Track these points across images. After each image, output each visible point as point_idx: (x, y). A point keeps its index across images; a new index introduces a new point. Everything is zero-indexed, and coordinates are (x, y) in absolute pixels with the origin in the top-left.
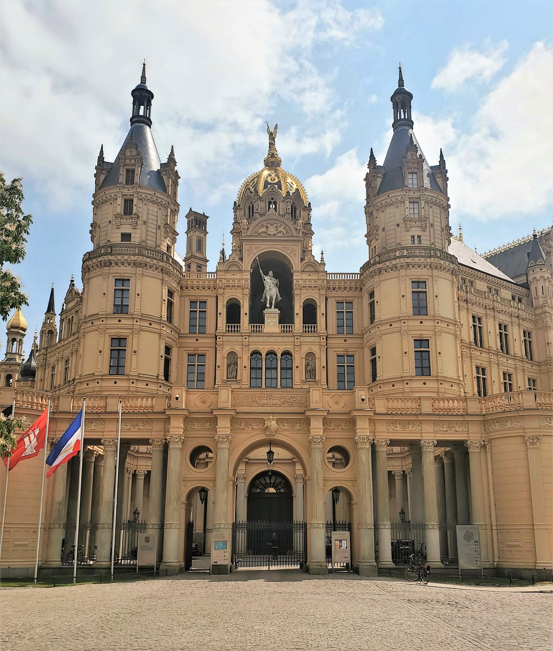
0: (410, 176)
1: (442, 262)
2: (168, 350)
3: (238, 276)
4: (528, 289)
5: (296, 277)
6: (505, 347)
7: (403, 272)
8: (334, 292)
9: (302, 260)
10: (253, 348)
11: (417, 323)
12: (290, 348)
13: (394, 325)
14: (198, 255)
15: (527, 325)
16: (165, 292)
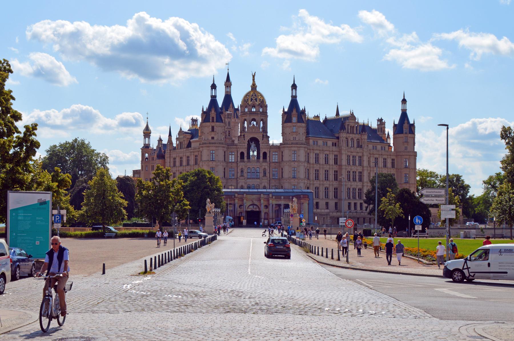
0: (294, 118)
1: (301, 145)
2: (224, 169)
3: (244, 144)
4: (339, 139)
5: (261, 145)
6: (327, 161)
7: (290, 148)
8: (272, 150)
9: (263, 140)
10: (248, 167)
11: (293, 163)
12: (259, 166)
13: (287, 163)
14: (229, 127)
15: (336, 153)
16: (224, 153)
